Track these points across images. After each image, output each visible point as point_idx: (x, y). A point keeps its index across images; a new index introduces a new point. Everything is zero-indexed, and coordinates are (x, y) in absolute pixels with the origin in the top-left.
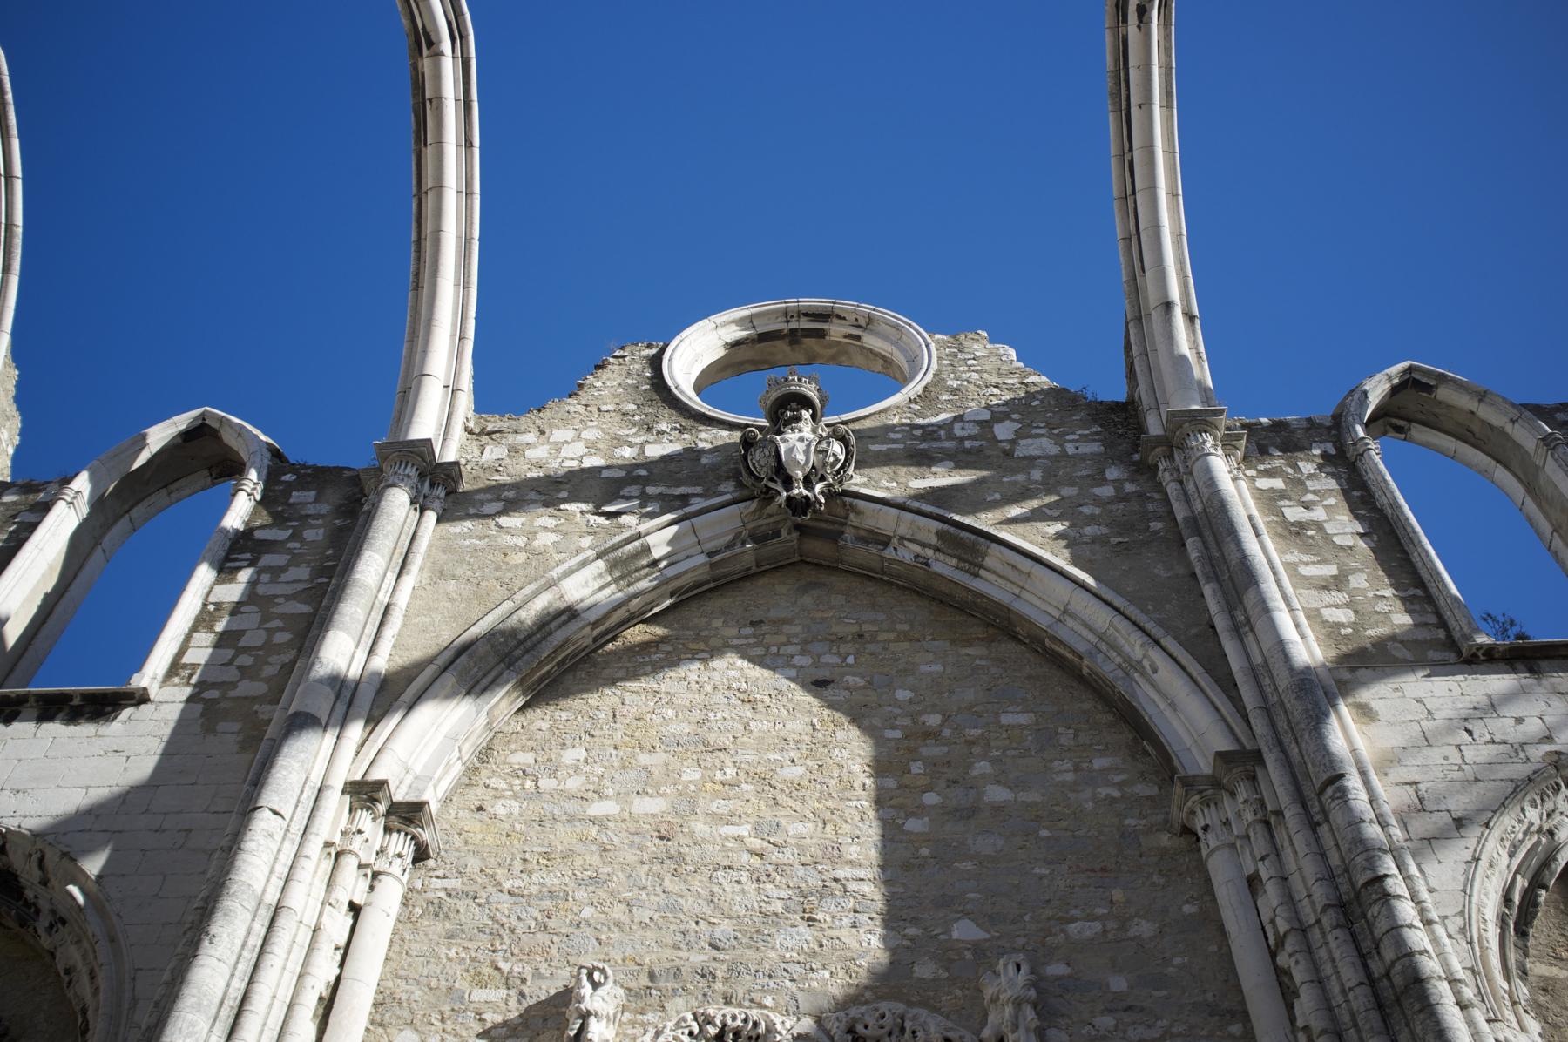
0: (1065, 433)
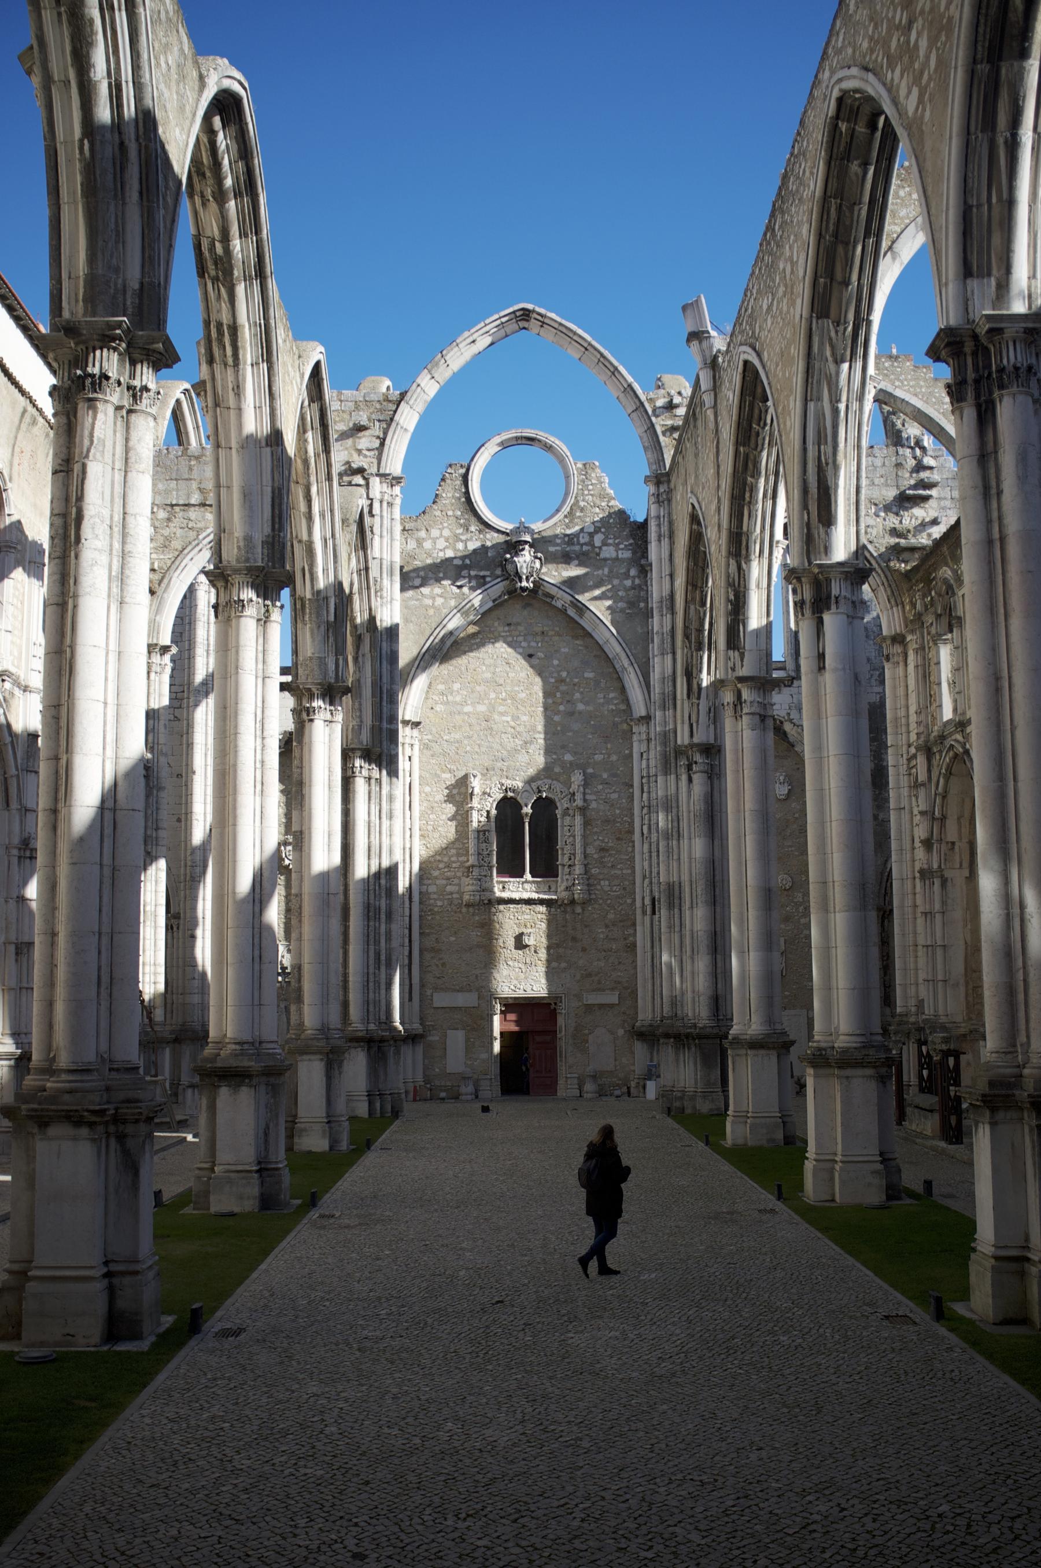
0: (619, 544)
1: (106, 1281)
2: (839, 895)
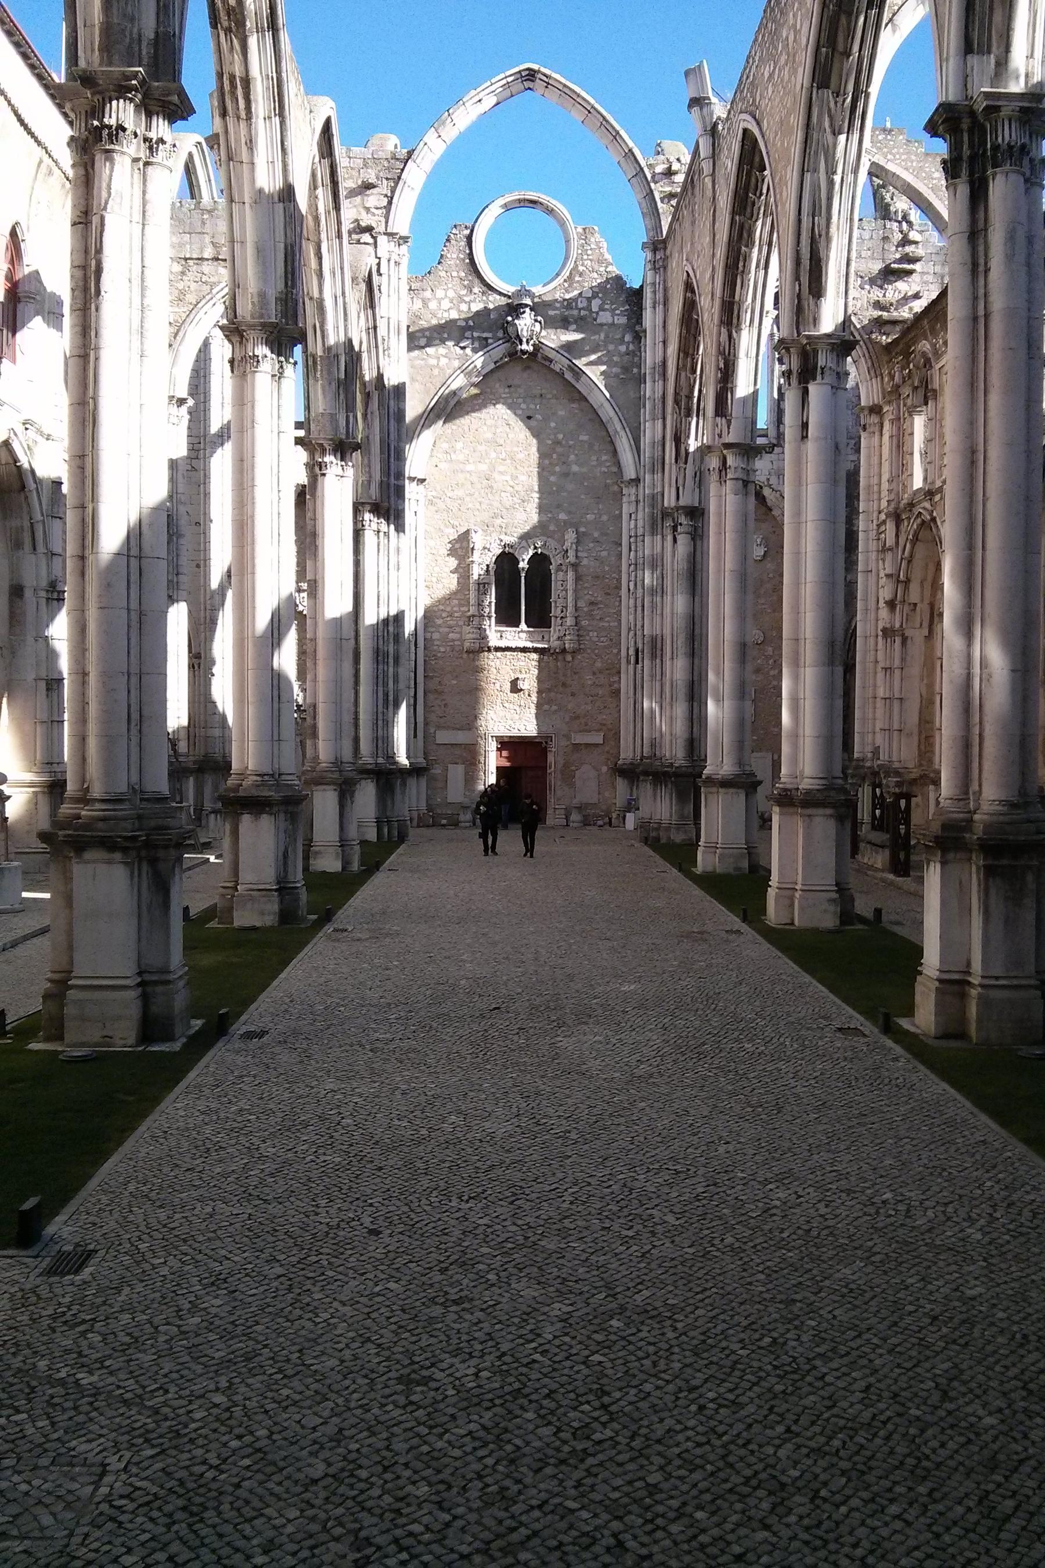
2: (810, 652)
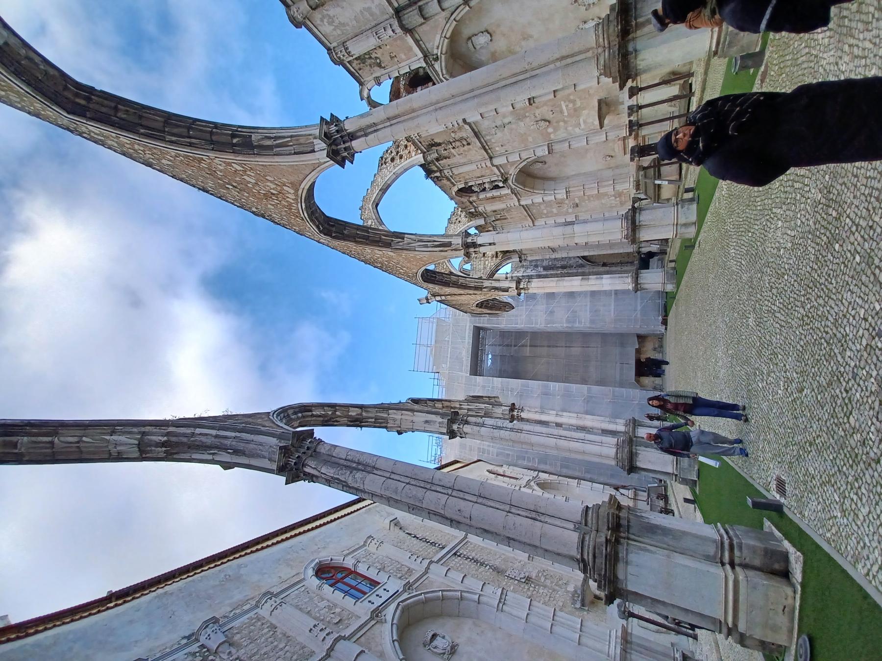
1: (738, 569)
